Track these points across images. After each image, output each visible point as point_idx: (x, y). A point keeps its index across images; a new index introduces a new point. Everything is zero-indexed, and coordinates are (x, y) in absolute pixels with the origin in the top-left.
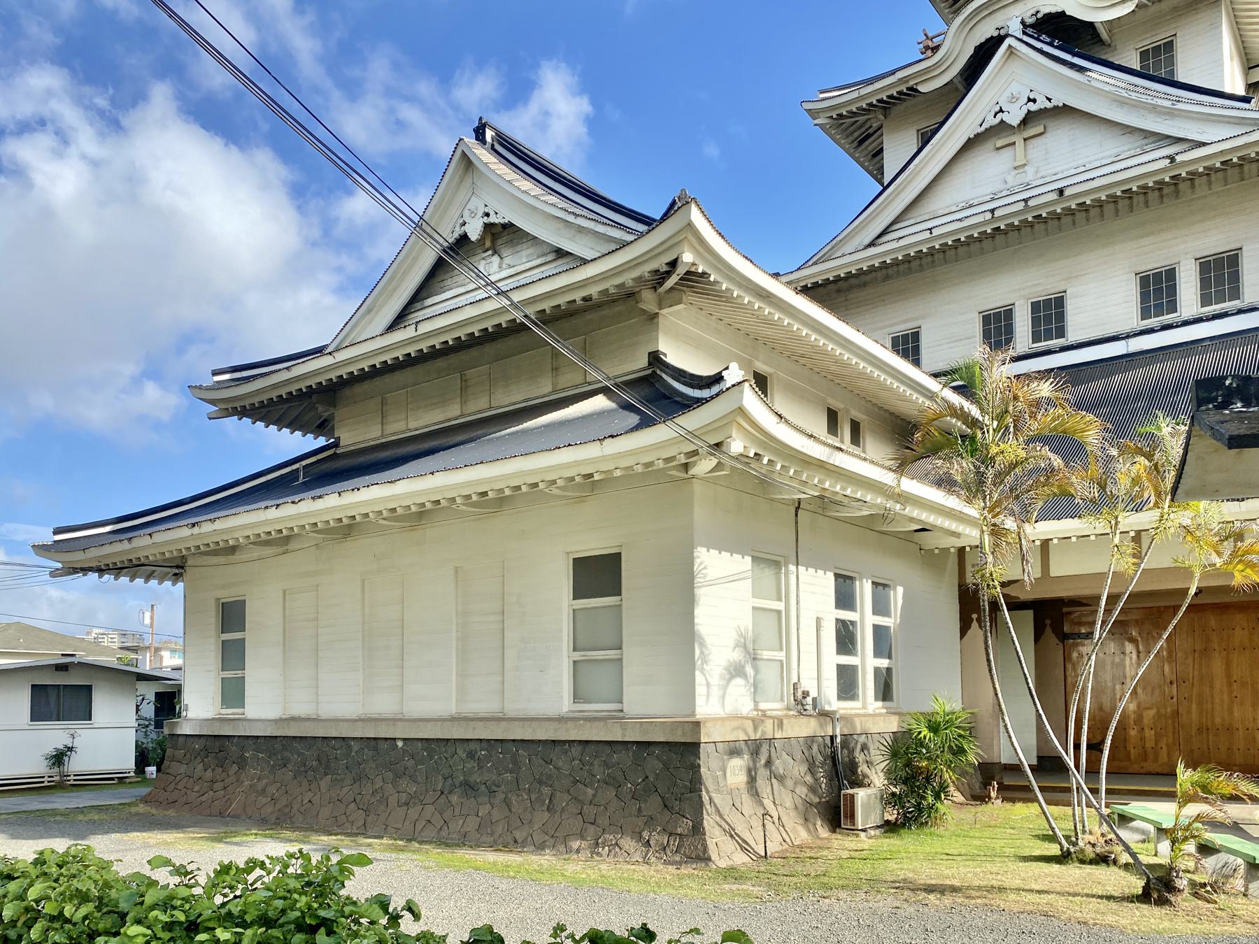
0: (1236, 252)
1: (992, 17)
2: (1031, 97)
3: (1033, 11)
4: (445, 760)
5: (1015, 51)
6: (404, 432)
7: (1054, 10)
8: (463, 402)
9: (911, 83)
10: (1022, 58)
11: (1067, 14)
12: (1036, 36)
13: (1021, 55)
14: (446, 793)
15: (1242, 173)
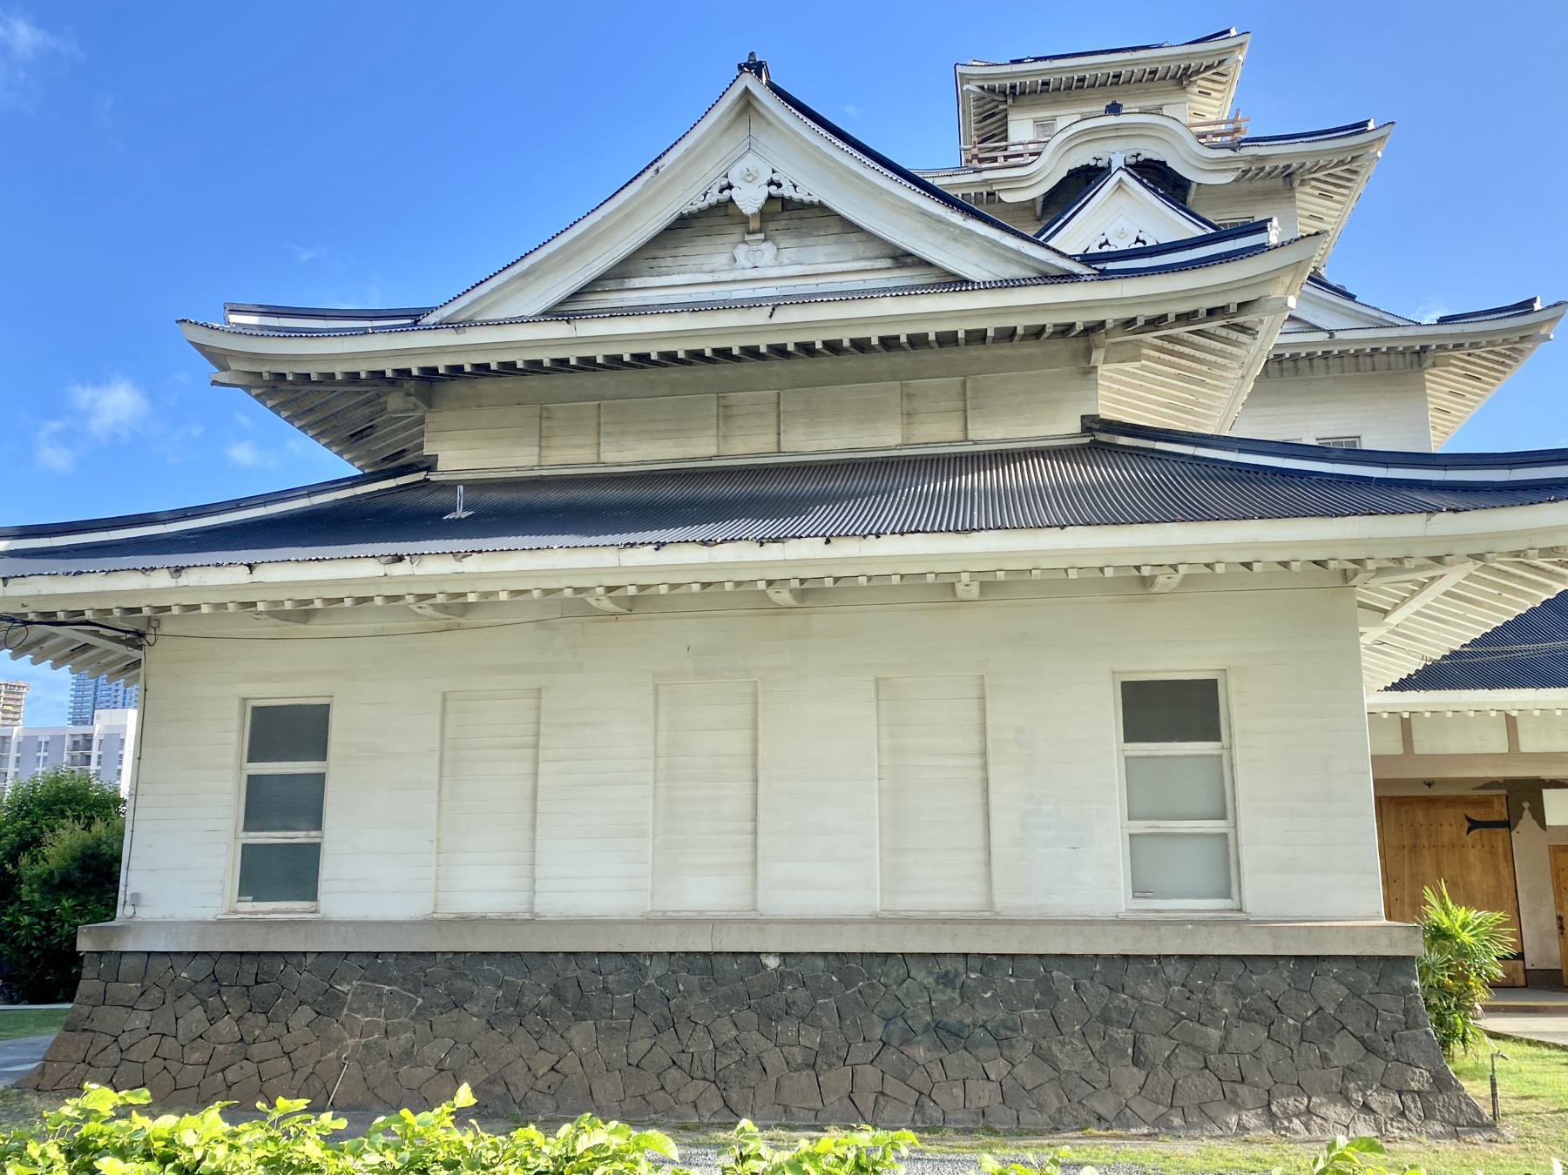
0: (1354, 439)
1: (1092, 144)
2: (1141, 238)
3: (1135, 153)
4: (883, 989)
5: (1122, 185)
6: (592, 465)
7: (1155, 158)
8: (724, 437)
9: (995, 188)
10: (1130, 196)
11: (1168, 165)
12: (1139, 177)
13: (1131, 192)
14: (895, 1042)
15: (1357, 363)
